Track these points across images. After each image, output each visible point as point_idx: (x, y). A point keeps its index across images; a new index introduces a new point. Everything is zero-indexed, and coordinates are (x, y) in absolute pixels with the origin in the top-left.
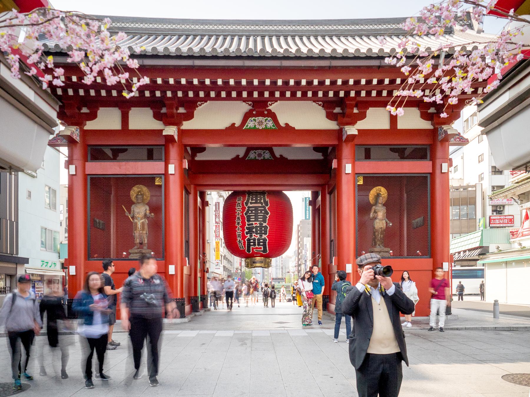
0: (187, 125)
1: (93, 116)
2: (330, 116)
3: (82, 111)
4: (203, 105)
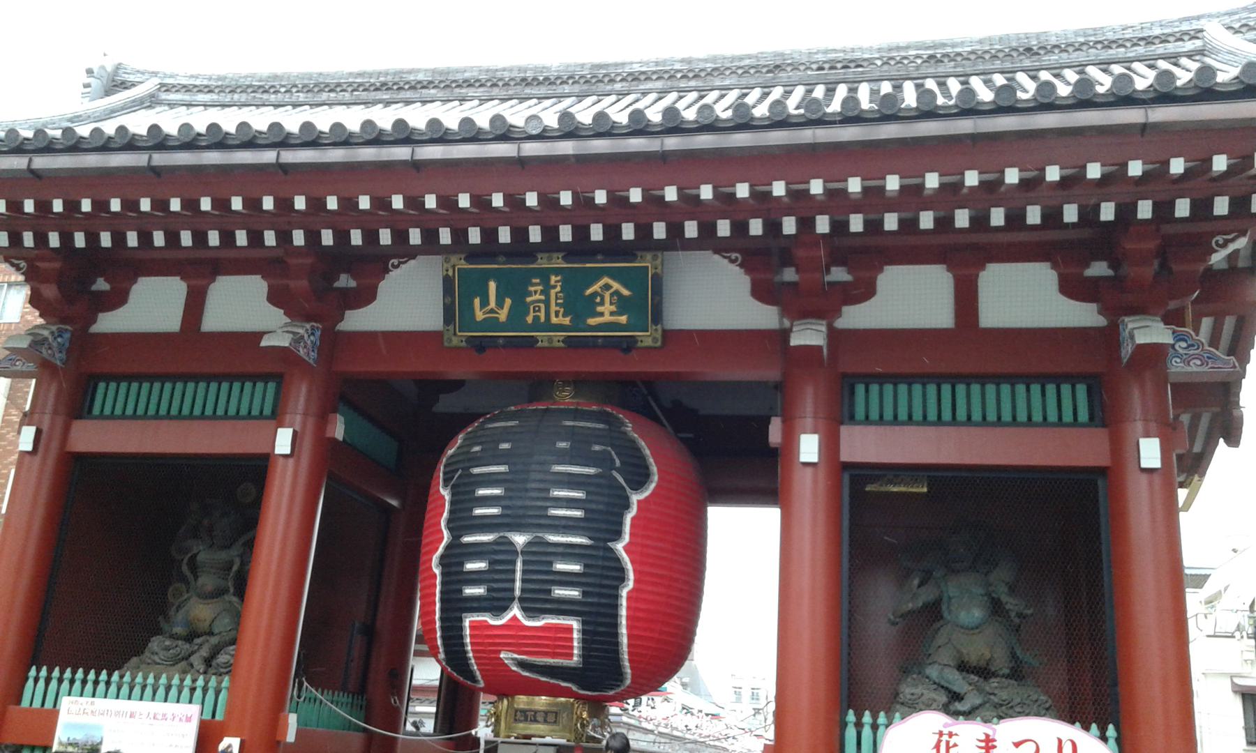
0: (357, 320)
1: (117, 299)
2: (762, 292)
3: (94, 288)
4: (403, 266)
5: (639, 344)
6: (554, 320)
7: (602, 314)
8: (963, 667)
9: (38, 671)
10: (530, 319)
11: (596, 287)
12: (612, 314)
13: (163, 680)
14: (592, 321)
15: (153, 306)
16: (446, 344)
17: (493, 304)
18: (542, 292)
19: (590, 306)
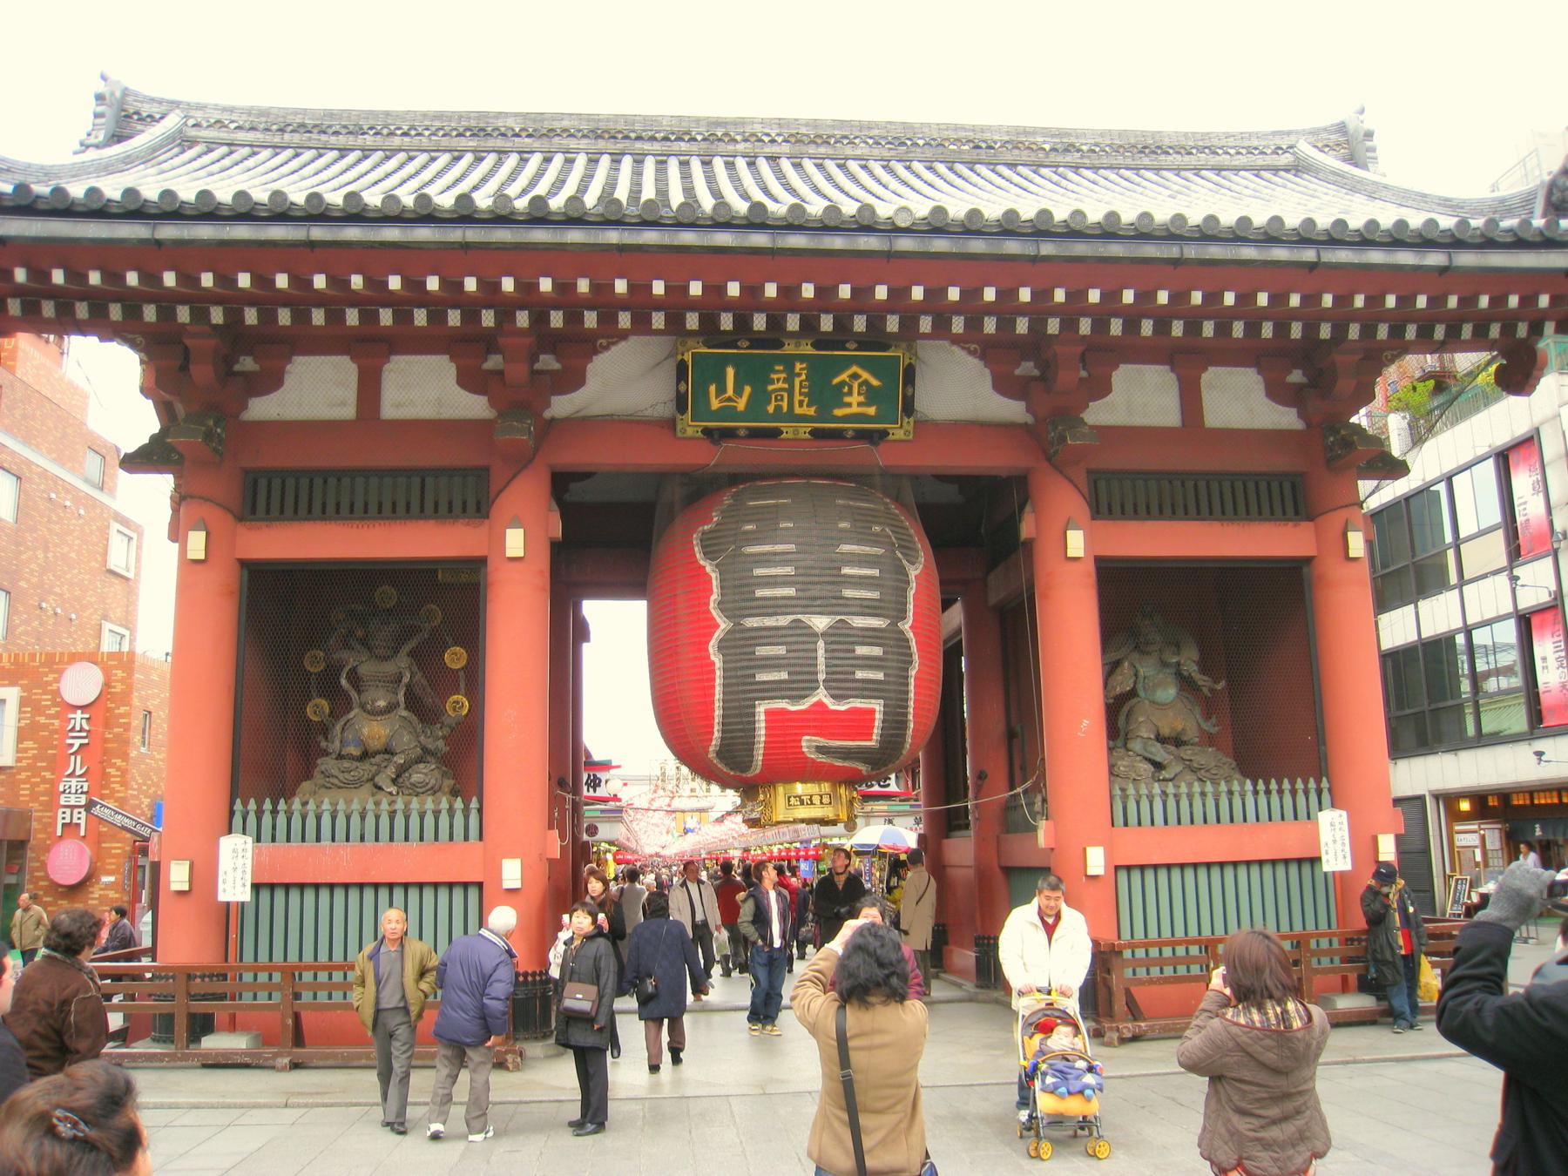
1: (271, 381)
2: (1005, 385)
3: (237, 368)
4: (614, 349)
5: (891, 437)
6: (798, 410)
7: (849, 405)
8: (1161, 739)
9: (245, 804)
10: (771, 409)
11: (844, 377)
12: (860, 404)
14: (839, 412)
15: (316, 389)
16: (679, 434)
17: (730, 392)
18: (785, 381)
19: (838, 395)
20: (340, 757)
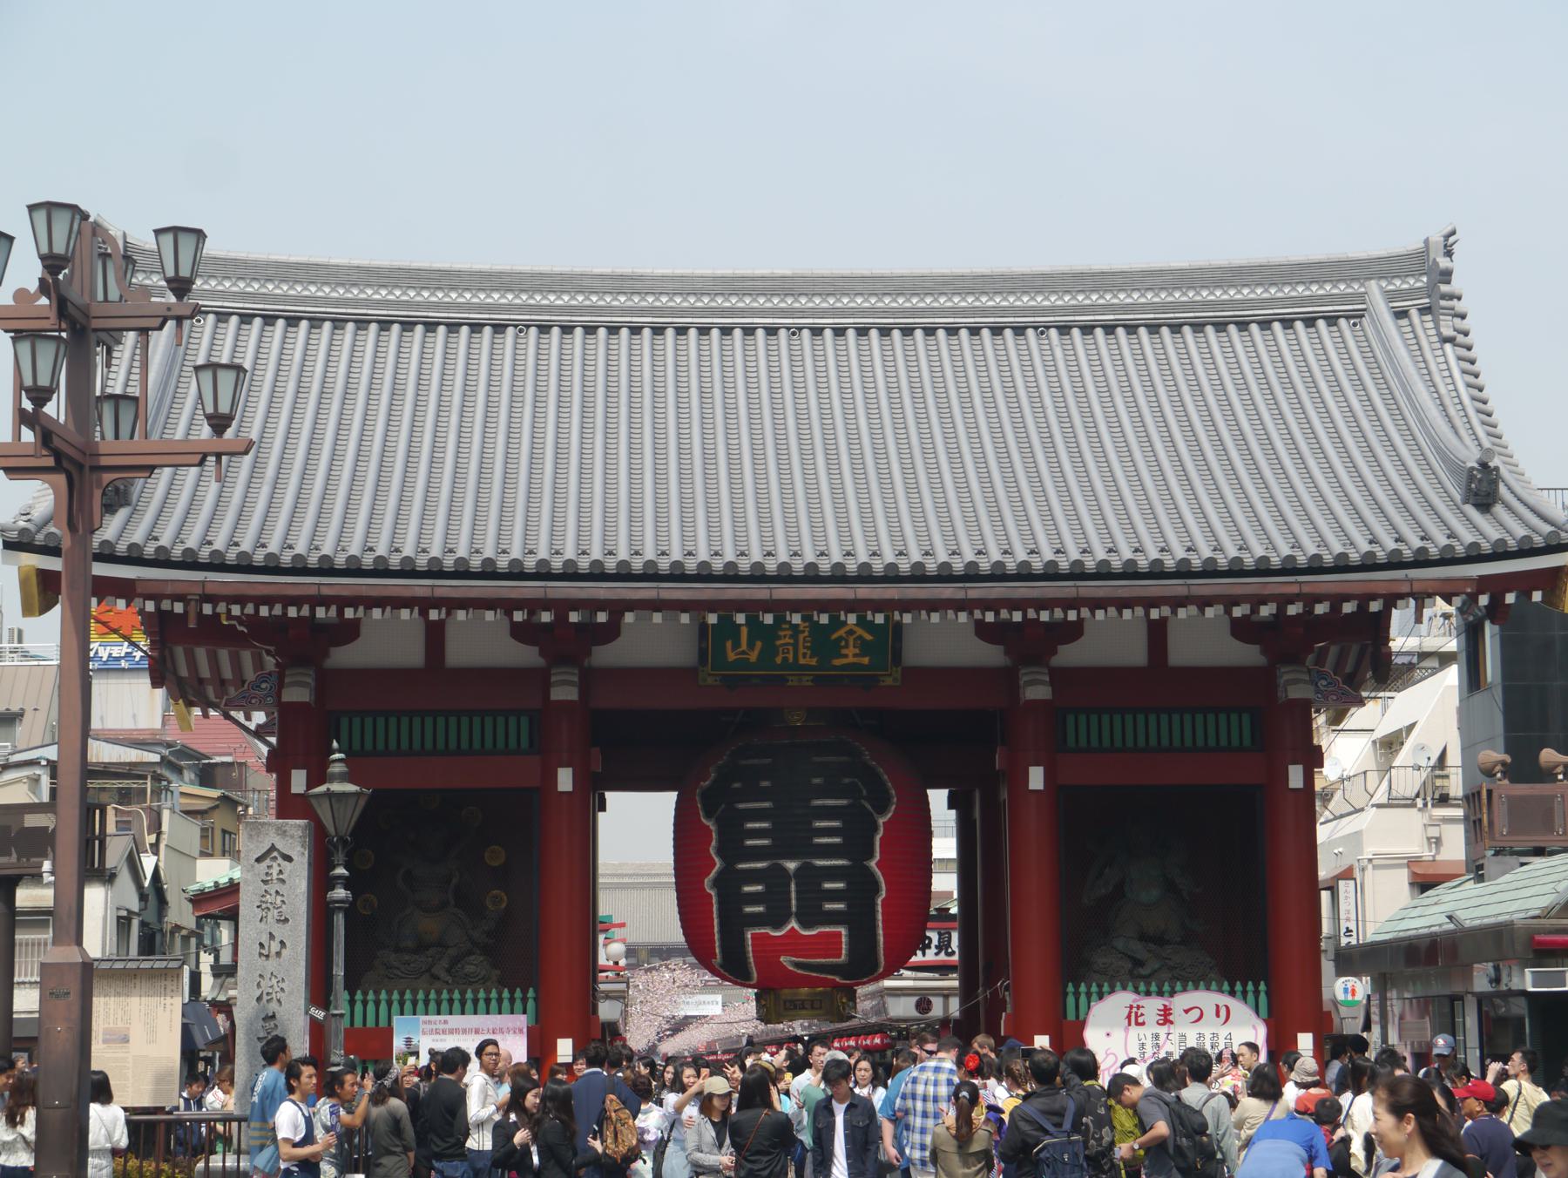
7: (846, 656)
8: (1143, 937)
10: (779, 660)
11: (842, 632)
13: (421, 996)
14: (837, 662)
17: (744, 647)
20: (398, 950)
